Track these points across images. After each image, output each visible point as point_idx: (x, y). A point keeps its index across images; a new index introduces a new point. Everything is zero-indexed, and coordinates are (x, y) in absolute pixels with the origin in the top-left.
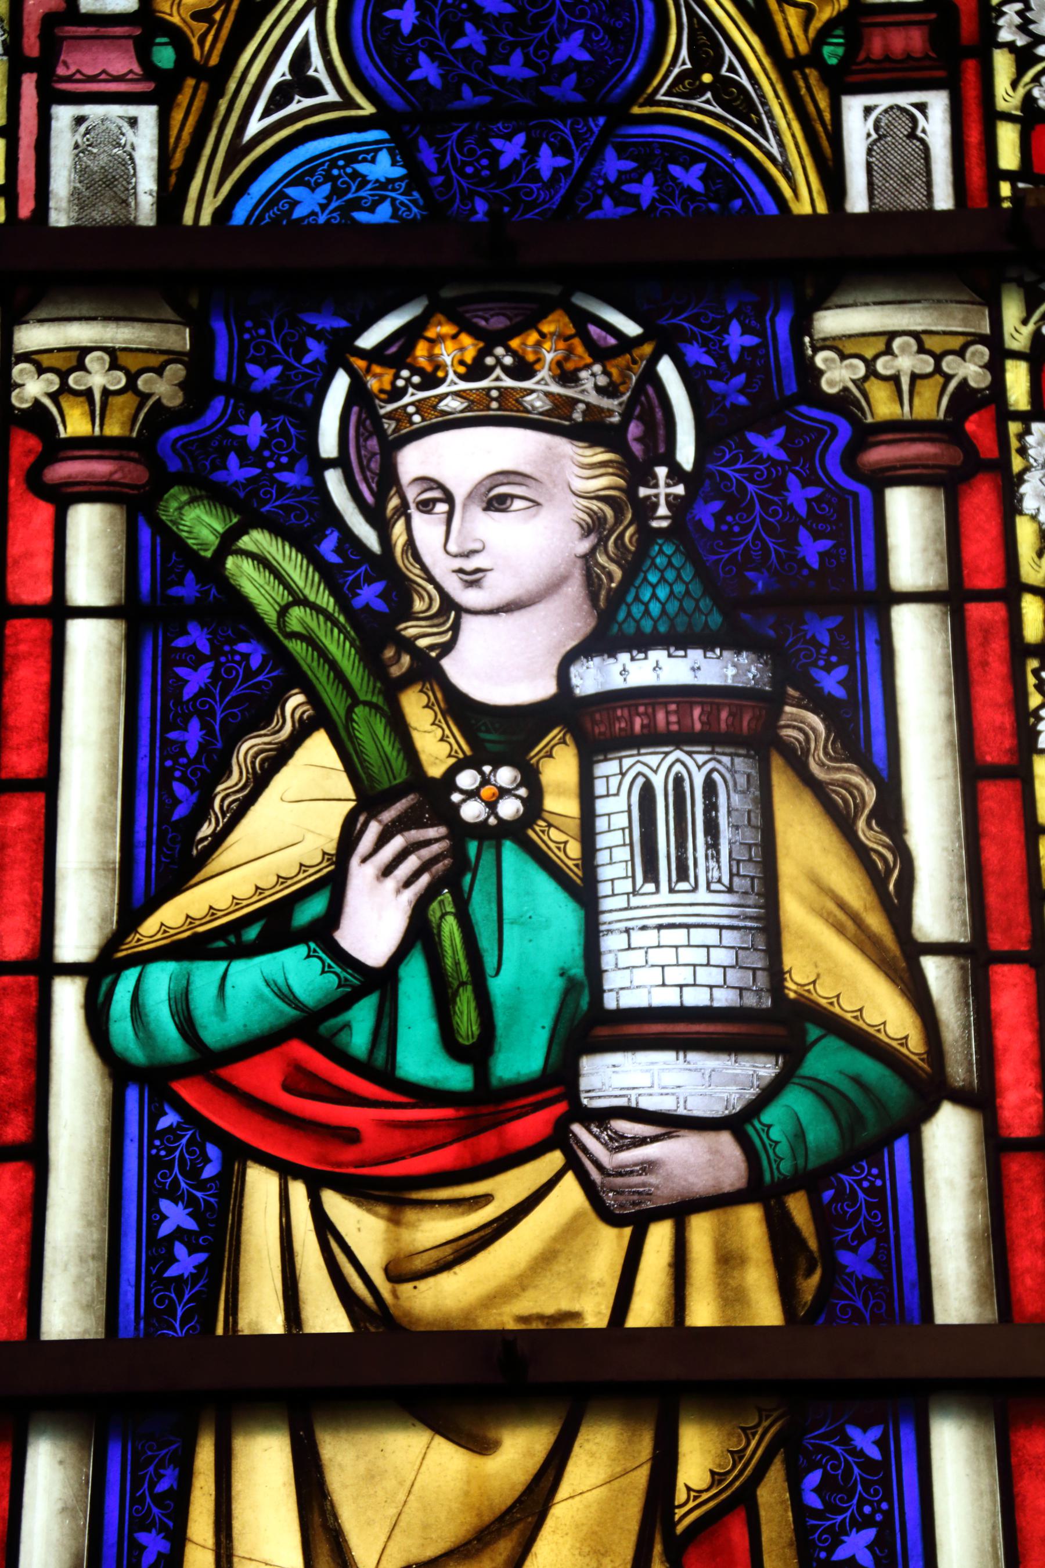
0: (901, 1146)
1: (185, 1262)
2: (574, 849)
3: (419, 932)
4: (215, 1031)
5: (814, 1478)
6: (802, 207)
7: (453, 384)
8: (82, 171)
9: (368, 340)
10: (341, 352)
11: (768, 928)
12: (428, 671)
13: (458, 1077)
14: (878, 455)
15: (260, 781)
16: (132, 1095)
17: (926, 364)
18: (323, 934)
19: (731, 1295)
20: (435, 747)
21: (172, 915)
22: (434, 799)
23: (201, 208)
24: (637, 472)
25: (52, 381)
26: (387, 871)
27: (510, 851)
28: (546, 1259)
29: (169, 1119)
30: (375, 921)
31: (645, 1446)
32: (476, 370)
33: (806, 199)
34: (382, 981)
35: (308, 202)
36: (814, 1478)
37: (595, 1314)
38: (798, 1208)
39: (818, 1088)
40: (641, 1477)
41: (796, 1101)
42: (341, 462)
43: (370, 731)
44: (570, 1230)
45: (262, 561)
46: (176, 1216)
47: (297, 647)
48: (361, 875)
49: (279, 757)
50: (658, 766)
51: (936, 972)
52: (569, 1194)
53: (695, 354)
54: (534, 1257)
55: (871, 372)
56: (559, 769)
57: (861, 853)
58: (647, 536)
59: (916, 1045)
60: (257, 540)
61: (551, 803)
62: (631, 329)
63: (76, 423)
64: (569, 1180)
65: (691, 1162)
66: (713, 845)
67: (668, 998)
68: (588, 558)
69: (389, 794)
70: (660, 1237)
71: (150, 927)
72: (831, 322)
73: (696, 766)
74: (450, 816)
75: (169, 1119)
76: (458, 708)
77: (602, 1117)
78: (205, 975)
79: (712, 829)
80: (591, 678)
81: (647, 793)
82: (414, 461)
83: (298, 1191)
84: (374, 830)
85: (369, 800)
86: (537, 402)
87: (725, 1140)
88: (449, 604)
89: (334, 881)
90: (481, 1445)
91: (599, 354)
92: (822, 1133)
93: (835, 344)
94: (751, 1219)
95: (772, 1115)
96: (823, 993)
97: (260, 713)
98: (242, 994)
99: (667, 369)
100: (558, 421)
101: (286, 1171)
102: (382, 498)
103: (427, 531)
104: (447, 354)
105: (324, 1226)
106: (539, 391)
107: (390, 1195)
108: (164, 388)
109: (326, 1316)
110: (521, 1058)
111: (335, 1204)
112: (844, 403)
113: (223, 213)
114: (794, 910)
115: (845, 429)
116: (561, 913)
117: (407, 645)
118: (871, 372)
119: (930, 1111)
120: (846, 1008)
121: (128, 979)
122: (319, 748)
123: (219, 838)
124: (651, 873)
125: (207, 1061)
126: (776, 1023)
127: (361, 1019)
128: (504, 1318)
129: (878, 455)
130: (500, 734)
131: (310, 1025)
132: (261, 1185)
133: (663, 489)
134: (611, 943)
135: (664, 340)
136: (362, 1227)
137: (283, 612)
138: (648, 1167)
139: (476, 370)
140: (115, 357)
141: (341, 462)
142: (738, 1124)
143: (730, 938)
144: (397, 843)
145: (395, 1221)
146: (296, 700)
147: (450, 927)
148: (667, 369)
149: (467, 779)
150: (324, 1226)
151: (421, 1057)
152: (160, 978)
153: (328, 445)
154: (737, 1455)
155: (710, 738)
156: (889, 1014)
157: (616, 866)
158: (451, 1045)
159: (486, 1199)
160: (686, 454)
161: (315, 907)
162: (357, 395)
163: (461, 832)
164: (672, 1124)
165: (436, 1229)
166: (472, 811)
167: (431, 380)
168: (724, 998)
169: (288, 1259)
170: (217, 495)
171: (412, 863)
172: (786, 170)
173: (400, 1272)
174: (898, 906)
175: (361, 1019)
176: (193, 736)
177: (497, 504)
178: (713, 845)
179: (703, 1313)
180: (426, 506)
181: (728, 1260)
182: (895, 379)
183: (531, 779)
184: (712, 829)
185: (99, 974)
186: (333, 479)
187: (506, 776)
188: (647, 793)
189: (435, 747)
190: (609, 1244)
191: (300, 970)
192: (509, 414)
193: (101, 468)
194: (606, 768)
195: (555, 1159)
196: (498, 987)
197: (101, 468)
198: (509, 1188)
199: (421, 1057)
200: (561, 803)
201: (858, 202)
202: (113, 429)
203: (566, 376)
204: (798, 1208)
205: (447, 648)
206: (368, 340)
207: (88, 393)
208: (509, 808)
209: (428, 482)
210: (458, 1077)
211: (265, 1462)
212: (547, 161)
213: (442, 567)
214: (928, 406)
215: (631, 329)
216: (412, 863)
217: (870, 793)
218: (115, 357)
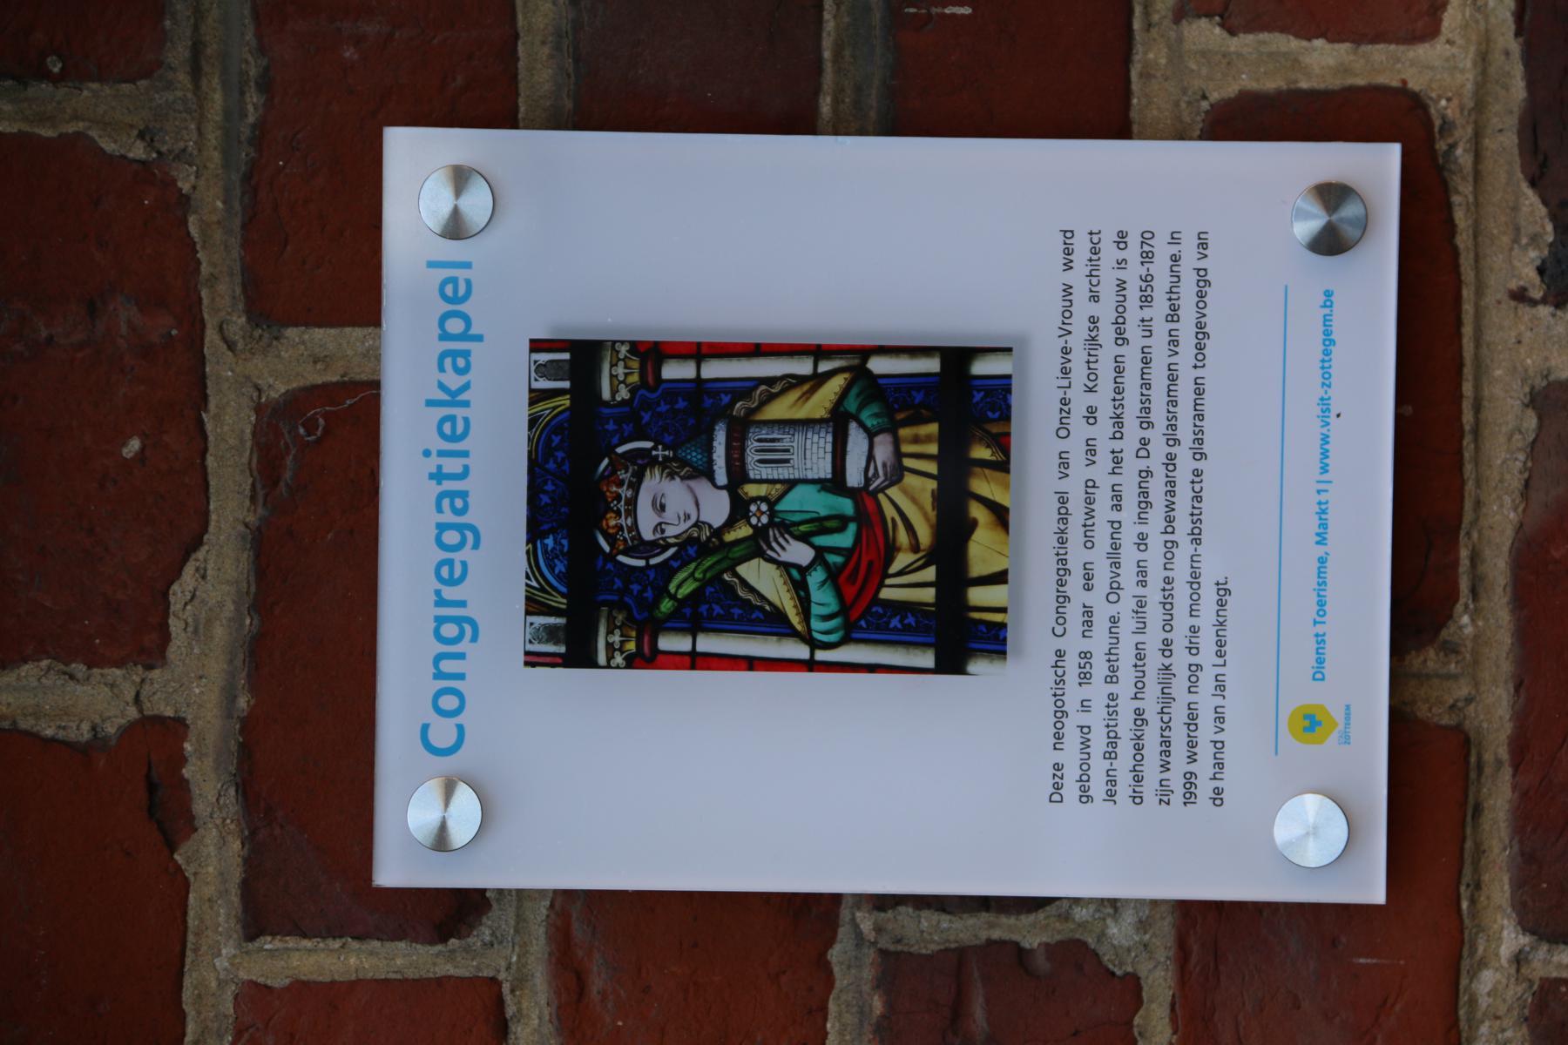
0: (881, 381)
1: (910, 620)
2: (778, 486)
3: (804, 538)
4: (833, 606)
5: (990, 414)
6: (568, 403)
7: (622, 521)
8: (548, 641)
9: (607, 548)
10: (611, 557)
11: (807, 424)
12: (718, 533)
13: (852, 527)
14: (650, 379)
15: (752, 590)
16: (854, 635)
17: (621, 364)
18: (804, 570)
19: (928, 439)
20: (743, 531)
21: (795, 620)
22: (760, 533)
23: (561, 602)
24: (653, 462)
25: (617, 654)
26: (783, 548)
27: (779, 507)
28: (914, 500)
29: (863, 623)
30: (799, 553)
31: (977, 470)
32: (618, 513)
33: (565, 402)
34: (820, 552)
35: (560, 567)
36: (990, 414)
37: (932, 485)
38: (900, 416)
39: (861, 408)
40: (987, 471)
41: (865, 415)
42: (647, 559)
43: (737, 552)
44: (905, 492)
45: (679, 586)
46: (895, 622)
47: (708, 575)
48: (785, 557)
49: (744, 583)
50: (751, 457)
51: (824, 367)
52: (893, 492)
53: (615, 440)
54: (912, 504)
55: (623, 382)
56: (752, 490)
57: (783, 391)
58: (675, 459)
59: (847, 375)
60: (672, 588)
61: (763, 493)
62: (606, 461)
63: (631, 646)
64: (888, 492)
65: (883, 451)
66: (778, 440)
67: (829, 457)
68: (683, 478)
69: (757, 547)
70: (908, 462)
71: (799, 628)
72: (606, 394)
73: (752, 445)
74: (766, 528)
75: (863, 623)
76: (730, 523)
77: (868, 481)
78: (815, 610)
79: (773, 440)
80: (721, 477)
81: (761, 461)
82: (648, 535)
83: (888, 581)
84: (770, 552)
85: (760, 554)
86: (629, 494)
87: (877, 439)
88: (696, 525)
89: (786, 567)
90: (974, 524)
91: (614, 472)
92: (874, 408)
93: (614, 392)
94: (904, 432)
95: (869, 423)
96: (829, 405)
97: (729, 588)
98: (823, 598)
99: (620, 450)
100: (636, 487)
101: (881, 585)
102: (659, 546)
103: (671, 531)
104: (612, 523)
105: (900, 573)
106: (626, 492)
107: (891, 550)
108: (620, 617)
109: (930, 574)
110: (846, 506)
111: (893, 569)
112: (633, 390)
113: (563, 595)
114: (801, 413)
115: (642, 392)
116: (800, 490)
117: (709, 539)
118: (623, 382)
119: (869, 372)
120: (833, 397)
121: (815, 635)
122: (742, 570)
123: (771, 604)
124: (787, 461)
125: (844, 610)
126: (838, 422)
127: (833, 559)
128: (932, 514)
129: (650, 379)
130: (739, 509)
131: (833, 576)
132: (885, 594)
133: (660, 453)
134: (810, 476)
135: (610, 451)
136: (902, 560)
137: (696, 580)
138: (884, 465)
139: (618, 513)
140: (610, 632)
141: (647, 559)
142: (871, 435)
143: (809, 435)
144: (774, 545)
145: (899, 550)
146: (726, 577)
147: (803, 528)
148: (620, 450)
149: (754, 521)
150: (900, 573)
151: (845, 539)
152: (816, 625)
153: (641, 563)
154: (981, 440)
155: (743, 439)
156: (837, 383)
157: (783, 473)
158: (841, 529)
159: (893, 520)
160: (648, 445)
161: (795, 573)
162: (626, 553)
163: (771, 524)
164: (870, 457)
165: (903, 537)
166: (765, 519)
167: (621, 528)
168: (830, 438)
169: (908, 584)
170: (656, 603)
171: (781, 540)
172: (554, 408)
173: (915, 548)
174: (799, 380)
175: (833, 559)
176: (737, 611)
177: (663, 508)
178: (778, 440)
179: (933, 449)
180: (663, 531)
181: (916, 440)
182: (626, 375)
183: (754, 500)
184: (773, 440)
185: (814, 645)
186: (653, 561)
187: (753, 508)
188: (761, 461)
189: (743, 531)
190: (909, 479)
191: (816, 577)
192: (632, 503)
193: (646, 639)
194: (751, 475)
195: (881, 496)
196: (823, 513)
197: (646, 639)
198: (890, 512)
199: (845, 539)
200: (762, 490)
201: (566, 384)
202: (634, 634)
203: (620, 484)
204: (900, 416)
205: (710, 526)
206: (607, 548)
207: (622, 642)
208: (764, 507)
209: (655, 530)
210: (852, 527)
211: (977, 596)
212: (549, 487)
213: (684, 527)
214: (635, 364)
215: (606, 461)
216: (781, 540)
217: (763, 387)
218: (610, 632)
